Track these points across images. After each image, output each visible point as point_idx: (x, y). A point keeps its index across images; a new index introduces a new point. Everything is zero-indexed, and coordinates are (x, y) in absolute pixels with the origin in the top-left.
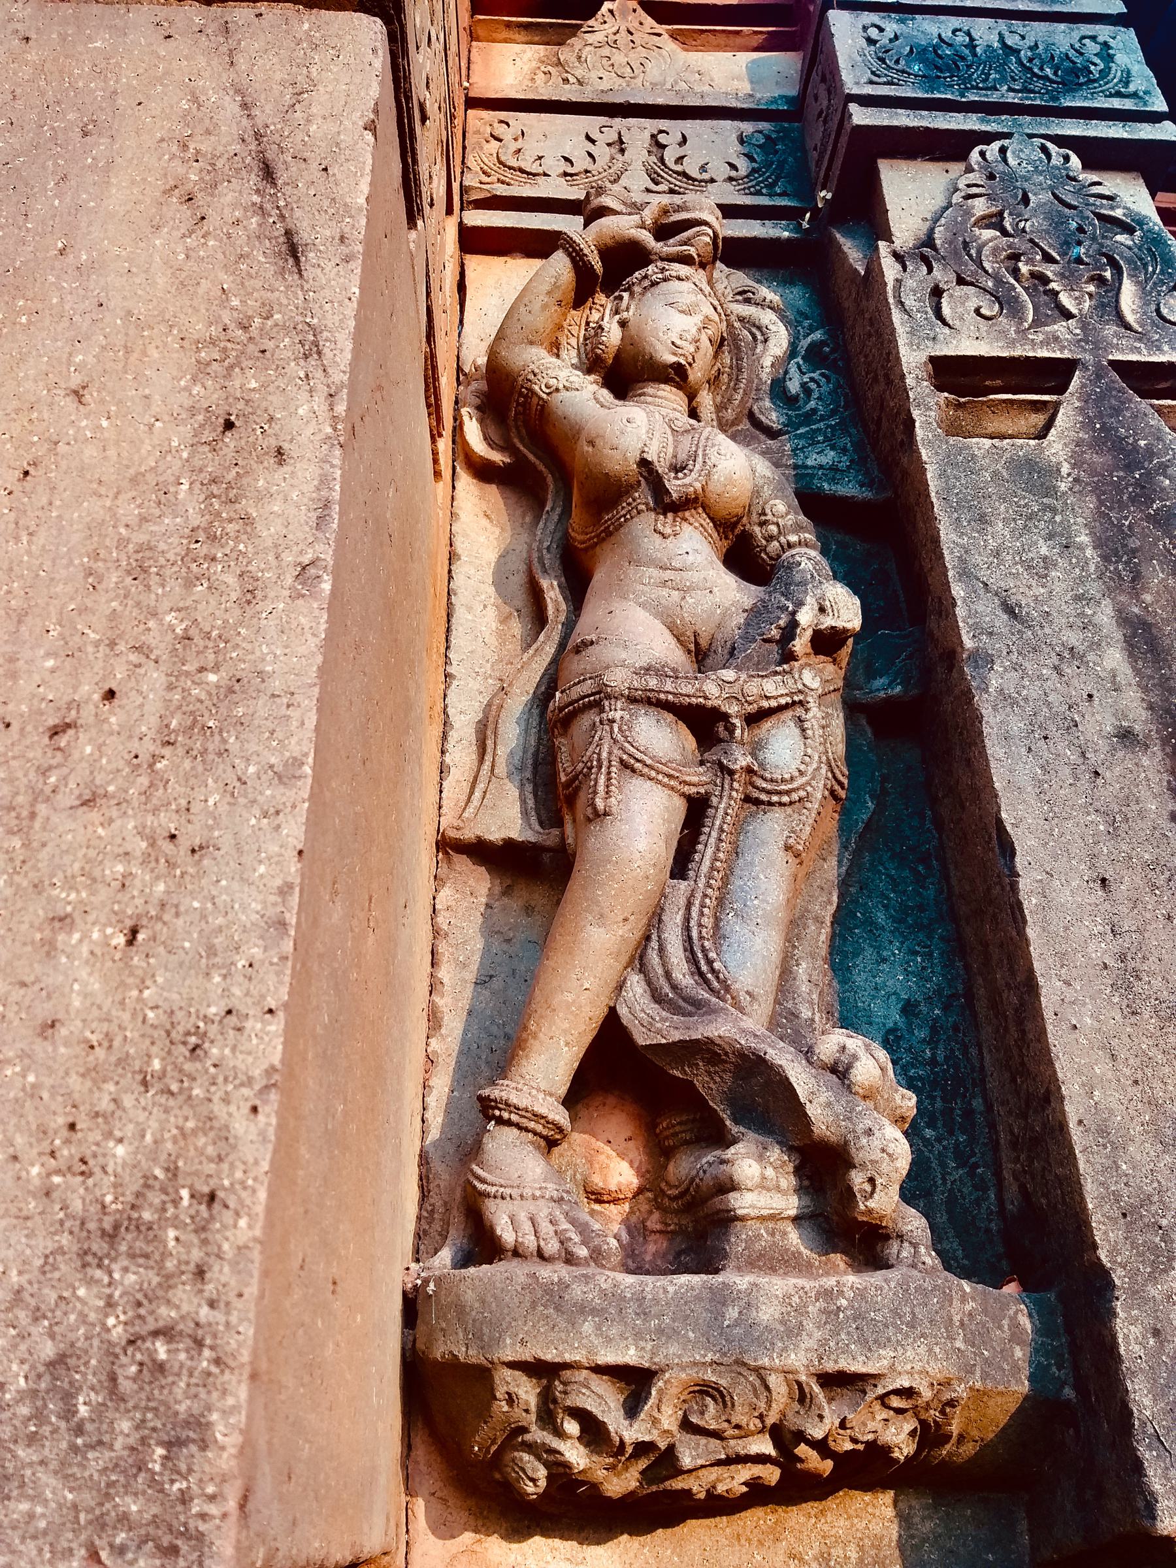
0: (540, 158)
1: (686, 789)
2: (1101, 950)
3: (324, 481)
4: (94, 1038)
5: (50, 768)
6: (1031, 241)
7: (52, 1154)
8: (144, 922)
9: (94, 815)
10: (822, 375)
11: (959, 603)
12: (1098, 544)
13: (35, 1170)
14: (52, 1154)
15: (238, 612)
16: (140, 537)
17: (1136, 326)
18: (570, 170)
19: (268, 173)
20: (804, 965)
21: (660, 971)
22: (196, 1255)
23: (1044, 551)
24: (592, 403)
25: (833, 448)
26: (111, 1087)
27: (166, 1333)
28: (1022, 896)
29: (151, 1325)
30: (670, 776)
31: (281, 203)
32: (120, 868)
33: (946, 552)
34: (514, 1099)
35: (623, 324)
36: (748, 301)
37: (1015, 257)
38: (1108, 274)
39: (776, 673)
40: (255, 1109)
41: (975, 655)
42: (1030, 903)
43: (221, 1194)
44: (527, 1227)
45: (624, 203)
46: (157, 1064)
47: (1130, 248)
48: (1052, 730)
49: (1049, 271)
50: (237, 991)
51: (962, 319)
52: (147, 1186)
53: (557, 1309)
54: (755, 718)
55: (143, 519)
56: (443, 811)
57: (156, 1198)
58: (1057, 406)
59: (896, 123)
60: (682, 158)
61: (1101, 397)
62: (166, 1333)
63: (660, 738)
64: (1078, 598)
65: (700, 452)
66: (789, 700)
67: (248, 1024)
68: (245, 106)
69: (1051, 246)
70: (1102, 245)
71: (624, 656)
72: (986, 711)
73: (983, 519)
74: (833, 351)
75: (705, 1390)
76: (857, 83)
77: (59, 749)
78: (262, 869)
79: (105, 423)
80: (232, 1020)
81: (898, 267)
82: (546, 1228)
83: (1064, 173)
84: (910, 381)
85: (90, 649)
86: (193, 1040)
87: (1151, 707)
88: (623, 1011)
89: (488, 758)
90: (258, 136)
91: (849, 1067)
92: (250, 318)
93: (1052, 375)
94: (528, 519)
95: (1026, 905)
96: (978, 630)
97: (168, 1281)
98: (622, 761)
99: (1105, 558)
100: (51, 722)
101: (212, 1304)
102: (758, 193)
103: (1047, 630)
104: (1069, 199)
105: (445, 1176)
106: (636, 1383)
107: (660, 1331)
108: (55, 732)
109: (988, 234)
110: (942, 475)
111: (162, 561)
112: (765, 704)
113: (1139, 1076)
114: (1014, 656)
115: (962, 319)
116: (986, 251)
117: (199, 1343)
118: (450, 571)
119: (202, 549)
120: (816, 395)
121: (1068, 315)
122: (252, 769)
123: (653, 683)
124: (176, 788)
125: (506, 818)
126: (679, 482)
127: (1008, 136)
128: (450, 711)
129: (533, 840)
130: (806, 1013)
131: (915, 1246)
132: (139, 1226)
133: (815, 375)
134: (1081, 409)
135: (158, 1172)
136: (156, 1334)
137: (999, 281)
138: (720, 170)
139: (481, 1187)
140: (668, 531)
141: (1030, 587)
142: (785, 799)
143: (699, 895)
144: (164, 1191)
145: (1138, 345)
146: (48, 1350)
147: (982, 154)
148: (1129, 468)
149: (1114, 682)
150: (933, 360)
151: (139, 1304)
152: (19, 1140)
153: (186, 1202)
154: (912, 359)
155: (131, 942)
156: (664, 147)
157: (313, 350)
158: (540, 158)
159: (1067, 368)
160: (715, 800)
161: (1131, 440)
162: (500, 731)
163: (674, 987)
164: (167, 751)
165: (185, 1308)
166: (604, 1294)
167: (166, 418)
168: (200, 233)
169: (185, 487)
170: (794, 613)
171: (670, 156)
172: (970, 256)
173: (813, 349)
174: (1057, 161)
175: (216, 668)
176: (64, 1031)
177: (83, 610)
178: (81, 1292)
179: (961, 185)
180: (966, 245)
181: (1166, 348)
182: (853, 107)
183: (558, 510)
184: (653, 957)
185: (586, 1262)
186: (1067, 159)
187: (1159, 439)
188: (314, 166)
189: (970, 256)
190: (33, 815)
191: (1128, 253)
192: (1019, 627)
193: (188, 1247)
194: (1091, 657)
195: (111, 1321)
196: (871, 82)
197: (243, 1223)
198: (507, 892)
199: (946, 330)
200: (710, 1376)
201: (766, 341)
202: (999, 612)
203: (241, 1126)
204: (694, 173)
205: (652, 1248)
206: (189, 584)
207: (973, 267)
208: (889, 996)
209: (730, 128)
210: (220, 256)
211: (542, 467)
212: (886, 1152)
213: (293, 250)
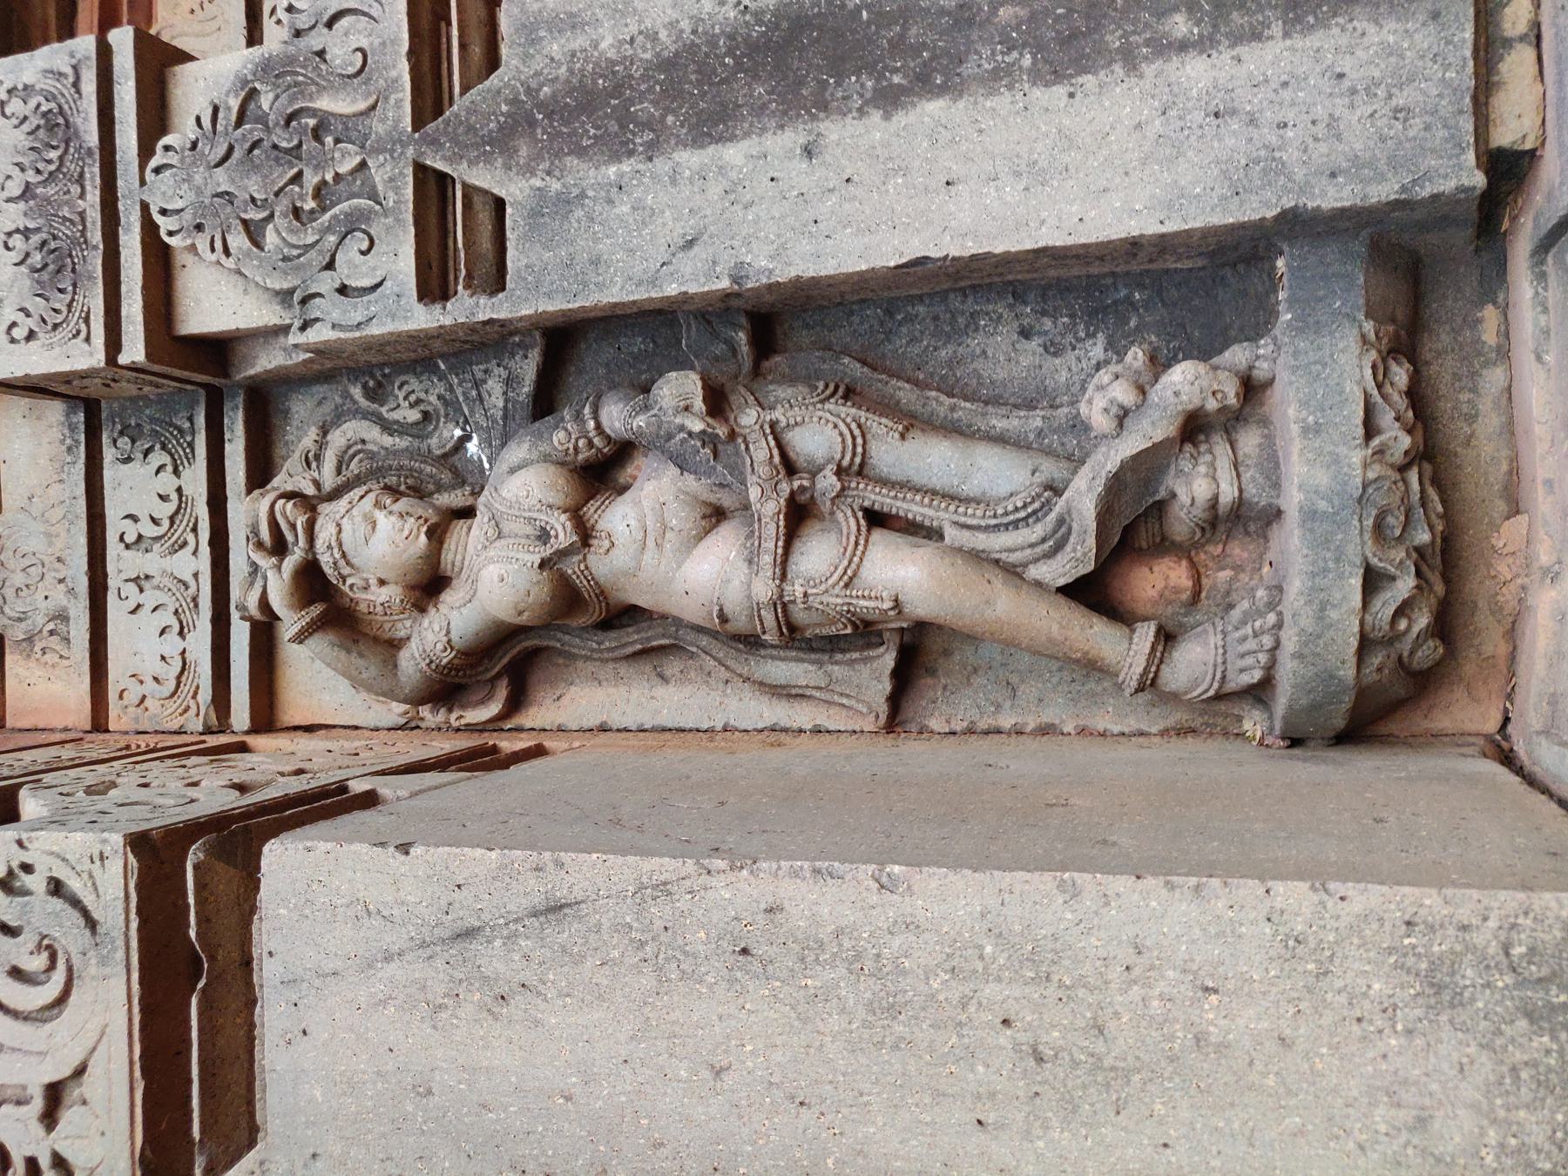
0: (163, 658)
1: (864, 529)
2: (1011, 191)
3: (795, 874)
4: (1292, 1010)
5: (1072, 1060)
6: (277, 194)
7: (1380, 1032)
8: (1198, 983)
9: (1112, 1025)
10: (400, 388)
11: (683, 289)
12: (616, 157)
13: (1393, 1042)
14: (1380, 1032)
15: (927, 935)
16: (861, 1013)
17: (371, 101)
18: (176, 628)
19: (469, 934)
20: (994, 422)
21: (1028, 551)
22: (1451, 931)
23: (625, 209)
24: (464, 611)
25: (485, 381)
26: (1329, 996)
27: (1506, 949)
28: (966, 254)
29: (1502, 958)
30: (857, 544)
31: (502, 921)
32: (1155, 1003)
33: (631, 298)
34: (1138, 669)
35: (382, 582)
36: (317, 457)
37: (297, 212)
38: (312, 122)
39: (747, 448)
40: (1342, 899)
41: (736, 280)
42: (970, 248)
43: (1407, 917)
44: (1249, 661)
45: (252, 584)
46: (1311, 966)
47: (277, 97)
48: (808, 215)
49: (311, 179)
50: (1252, 916)
51: (374, 269)
52: (1402, 967)
53: (1319, 637)
54: (790, 467)
55: (843, 1011)
56: (858, 729)
57: (1410, 961)
58: (465, 185)
59: (140, 318)
60: (152, 519)
61: (455, 141)
62: (1506, 949)
63: (818, 555)
64: (674, 182)
65: (527, 514)
66: (770, 438)
67: (1278, 906)
68: (388, 958)
69: (280, 176)
70: (277, 124)
71: (736, 583)
72: (793, 272)
73: (596, 262)
74: (373, 376)
75: (1379, 528)
76: (91, 354)
77: (1056, 1055)
78: (1154, 904)
79: (749, 1048)
80: (1275, 918)
81: (318, 325)
82: (1251, 645)
83: (187, 153)
84: (447, 321)
85: (966, 1040)
86: (1291, 943)
87: (782, 127)
88: (1062, 582)
89: (808, 693)
90: (424, 945)
91: (1122, 407)
92: (631, 940)
93: (433, 189)
94: (561, 661)
95: (974, 251)
96: (711, 274)
97: (1470, 948)
98: (847, 586)
99: (631, 153)
100: (1033, 1063)
101: (1485, 919)
102: (191, 445)
103: (708, 212)
104: (221, 150)
105: (1179, 715)
106: (1373, 581)
107: (1337, 560)
108: (1040, 1060)
109: (271, 238)
110: (549, 295)
111: (883, 994)
112: (777, 459)
113: (1121, 171)
114: (736, 243)
115: (374, 269)
116: (293, 240)
117: (1513, 926)
118: (618, 730)
119: (869, 965)
120: (422, 396)
121: (363, 165)
122: (1069, 916)
123: (767, 559)
124: (1087, 969)
125: (873, 675)
126: (561, 535)
127: (145, 207)
128: (760, 726)
129: (894, 654)
130: (1039, 423)
131: (1258, 357)
132: (1432, 970)
133: (401, 395)
134: (471, 163)
135: (1392, 960)
136: (1507, 954)
137: (328, 229)
138: (167, 482)
139: (1211, 693)
140: (606, 543)
141: (664, 224)
142: (859, 441)
143: (955, 518)
144: (1405, 955)
145: (392, 101)
146: (1523, 1024)
147: (171, 234)
148: (533, 124)
149: (759, 158)
150: (420, 299)
151: (1488, 967)
152: (1370, 1055)
153: (1413, 940)
154: (423, 318)
155: (1216, 991)
156: (140, 537)
157: (663, 888)
158: (163, 658)
159: (421, 170)
160: (866, 504)
161: (502, 119)
162: (783, 682)
163: (1044, 540)
164: (1055, 978)
165: (1489, 936)
166: (1309, 602)
167: (741, 1001)
168: (541, 988)
169: (809, 982)
170: (690, 434)
171: (150, 530)
172: (299, 256)
173: (371, 395)
174: (172, 158)
175: (981, 948)
176: (1288, 1032)
177: (931, 1050)
178: (1480, 1005)
179: (213, 257)
180: (285, 259)
181: (394, 74)
182: (123, 359)
183: (559, 635)
184: (1014, 558)
185: (1280, 614)
186: (167, 148)
187: (499, 92)
188: (457, 895)
189: (299, 256)
190: (1113, 1069)
191: (284, 99)
192: (705, 237)
193: (1445, 937)
194: (733, 175)
195: (1500, 984)
196: (88, 339)
197: (1428, 902)
198: (932, 672)
199: (388, 284)
200: (1369, 522)
201: (363, 442)
202: (692, 253)
203: (1357, 906)
204: (171, 507)
205: (1237, 551)
206: (904, 973)
207: (313, 254)
208: (1015, 350)
209: (111, 473)
210: (566, 969)
211: (515, 651)
212: (1185, 383)
213: (555, 909)
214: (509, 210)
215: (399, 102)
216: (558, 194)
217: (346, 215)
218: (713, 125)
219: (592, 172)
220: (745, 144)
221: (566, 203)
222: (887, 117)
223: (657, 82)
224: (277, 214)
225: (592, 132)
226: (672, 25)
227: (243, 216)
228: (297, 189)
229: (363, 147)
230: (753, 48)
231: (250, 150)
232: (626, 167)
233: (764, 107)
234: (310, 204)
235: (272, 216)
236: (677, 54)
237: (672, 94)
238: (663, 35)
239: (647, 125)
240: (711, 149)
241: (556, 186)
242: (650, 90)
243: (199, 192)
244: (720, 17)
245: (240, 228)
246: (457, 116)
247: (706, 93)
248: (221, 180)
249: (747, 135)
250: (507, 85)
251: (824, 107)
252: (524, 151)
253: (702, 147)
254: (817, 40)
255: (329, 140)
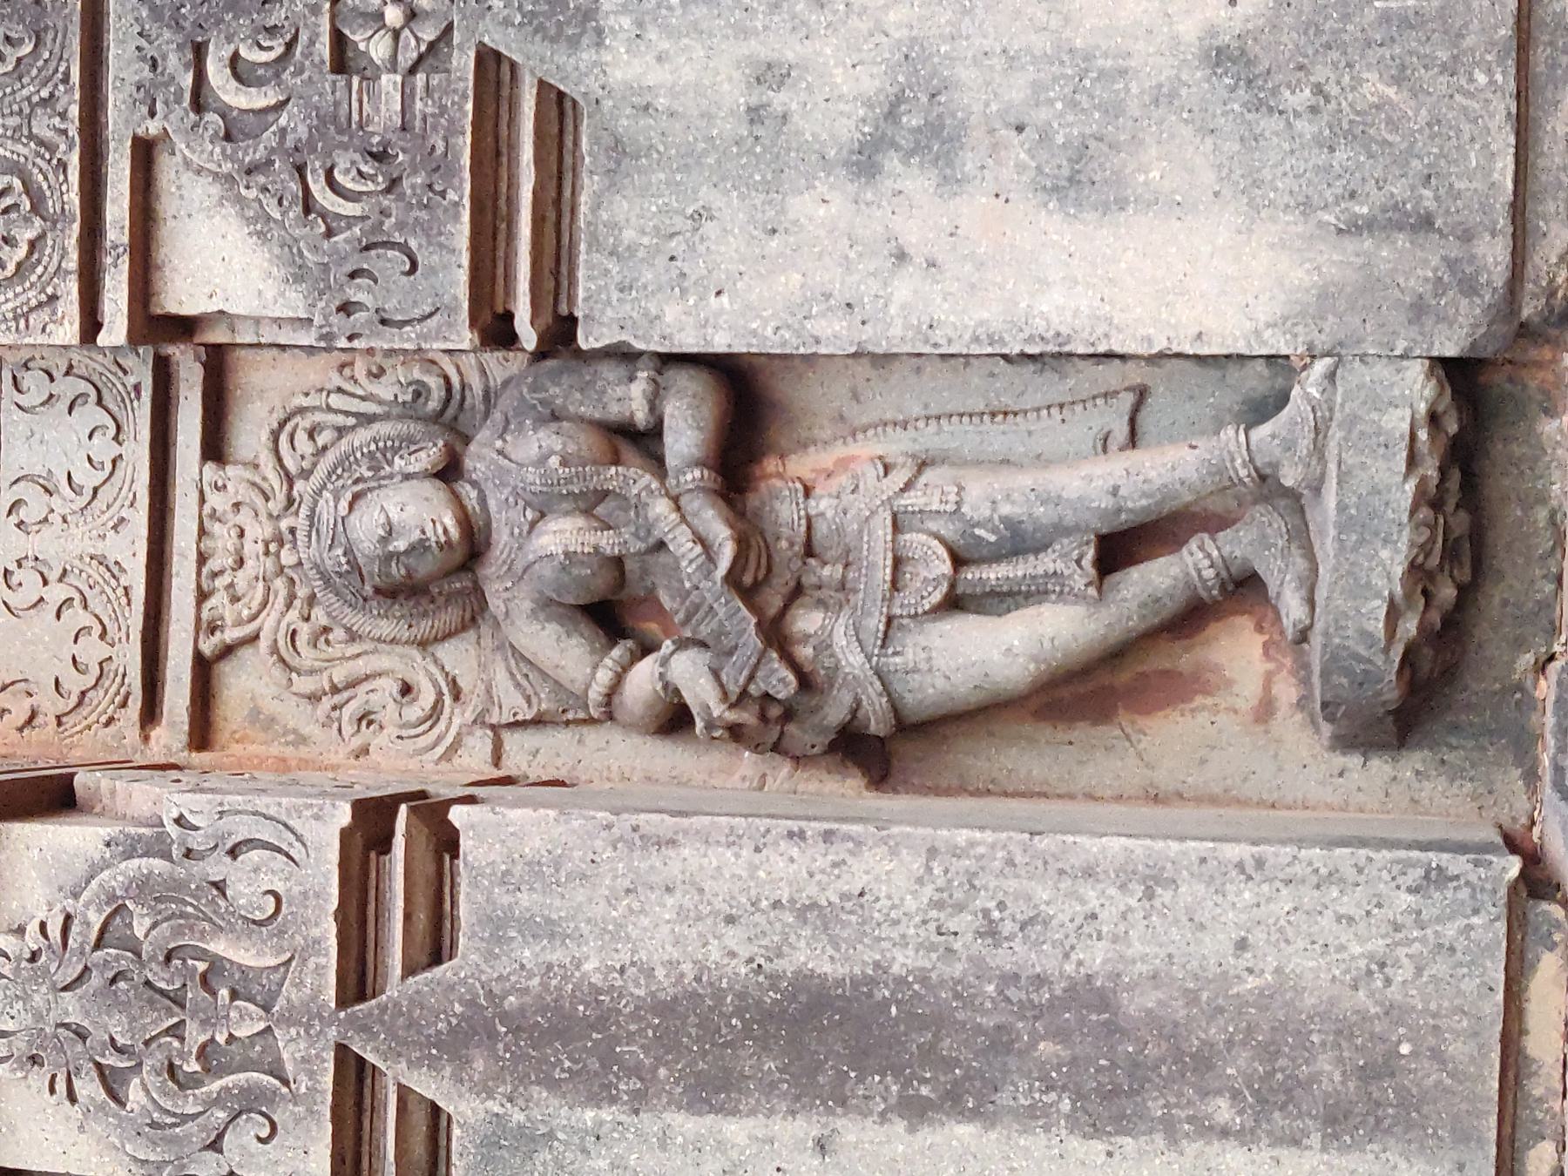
6: (147, 1043)
12: (594, 1101)
23: (603, 1164)
49: (196, 1036)
99: (613, 1100)
116: (168, 1105)
134: (410, 1064)
137: (216, 1102)
149: (764, 1142)
159: (342, 1050)
161: (454, 1021)
194: (734, 1155)
214: (456, 1132)
215: (319, 970)
216: (520, 1127)
217: (242, 1089)
218: (712, 1091)
219: (564, 1111)
220: (750, 1122)
221: (530, 1140)
222: (912, 1130)
223: (649, 1026)
224: (145, 1068)
225: (567, 1064)
226: (671, 964)
227: (98, 1058)
228: (176, 1044)
229: (267, 1008)
230: (768, 1016)
231: (113, 981)
232: (607, 1114)
233: (773, 1085)
234: (193, 1066)
235: (140, 1064)
236: (675, 999)
237: (667, 1043)
238: (660, 973)
239: (635, 1071)
240: (710, 1119)
241: (518, 1117)
242: (640, 1030)
243: (39, 1017)
244: (729, 970)
245: (94, 1074)
246: (397, 1004)
247: (705, 1053)
248: (72, 1008)
249: (753, 1112)
250: (463, 982)
251: (843, 1103)
252: (479, 1065)
253: (700, 1114)
254: (840, 1023)
255: (224, 993)
